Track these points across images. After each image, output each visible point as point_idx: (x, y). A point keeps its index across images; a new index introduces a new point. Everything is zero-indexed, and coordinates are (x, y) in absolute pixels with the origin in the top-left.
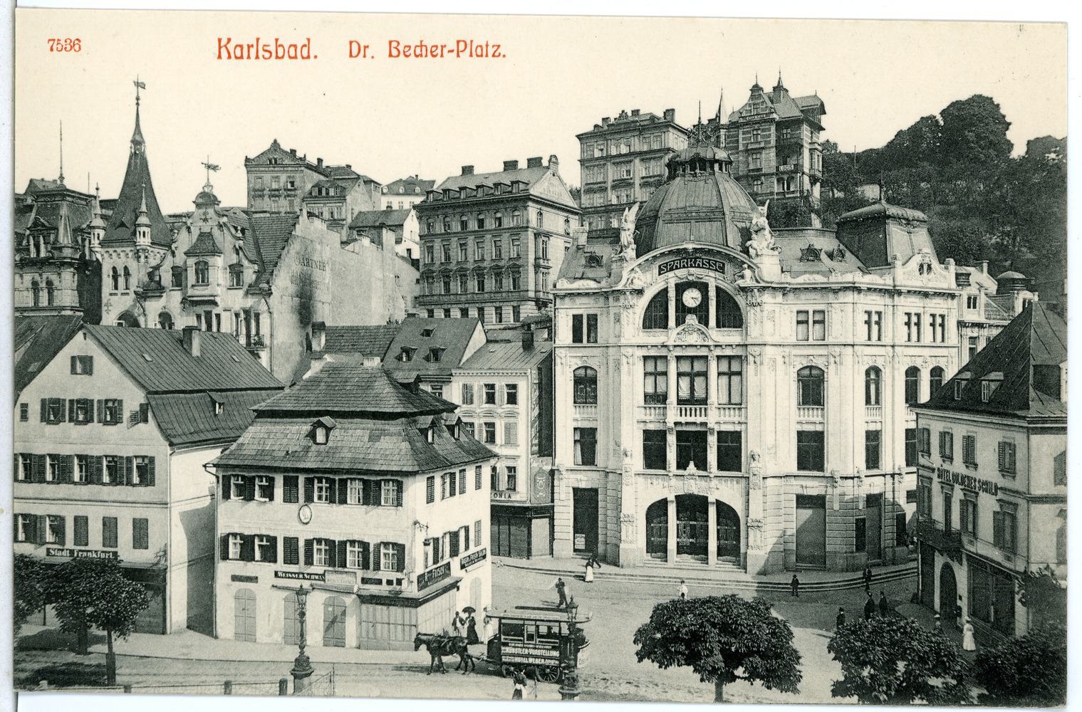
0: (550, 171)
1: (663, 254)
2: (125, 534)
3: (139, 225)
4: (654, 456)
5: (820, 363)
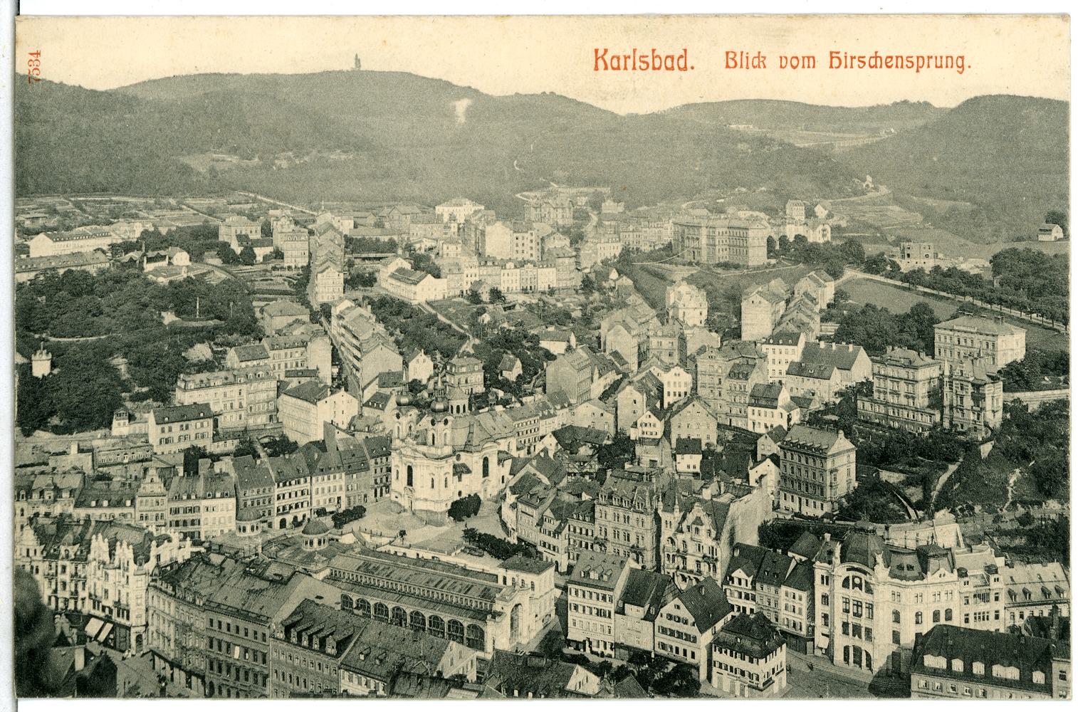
2: (689, 654)
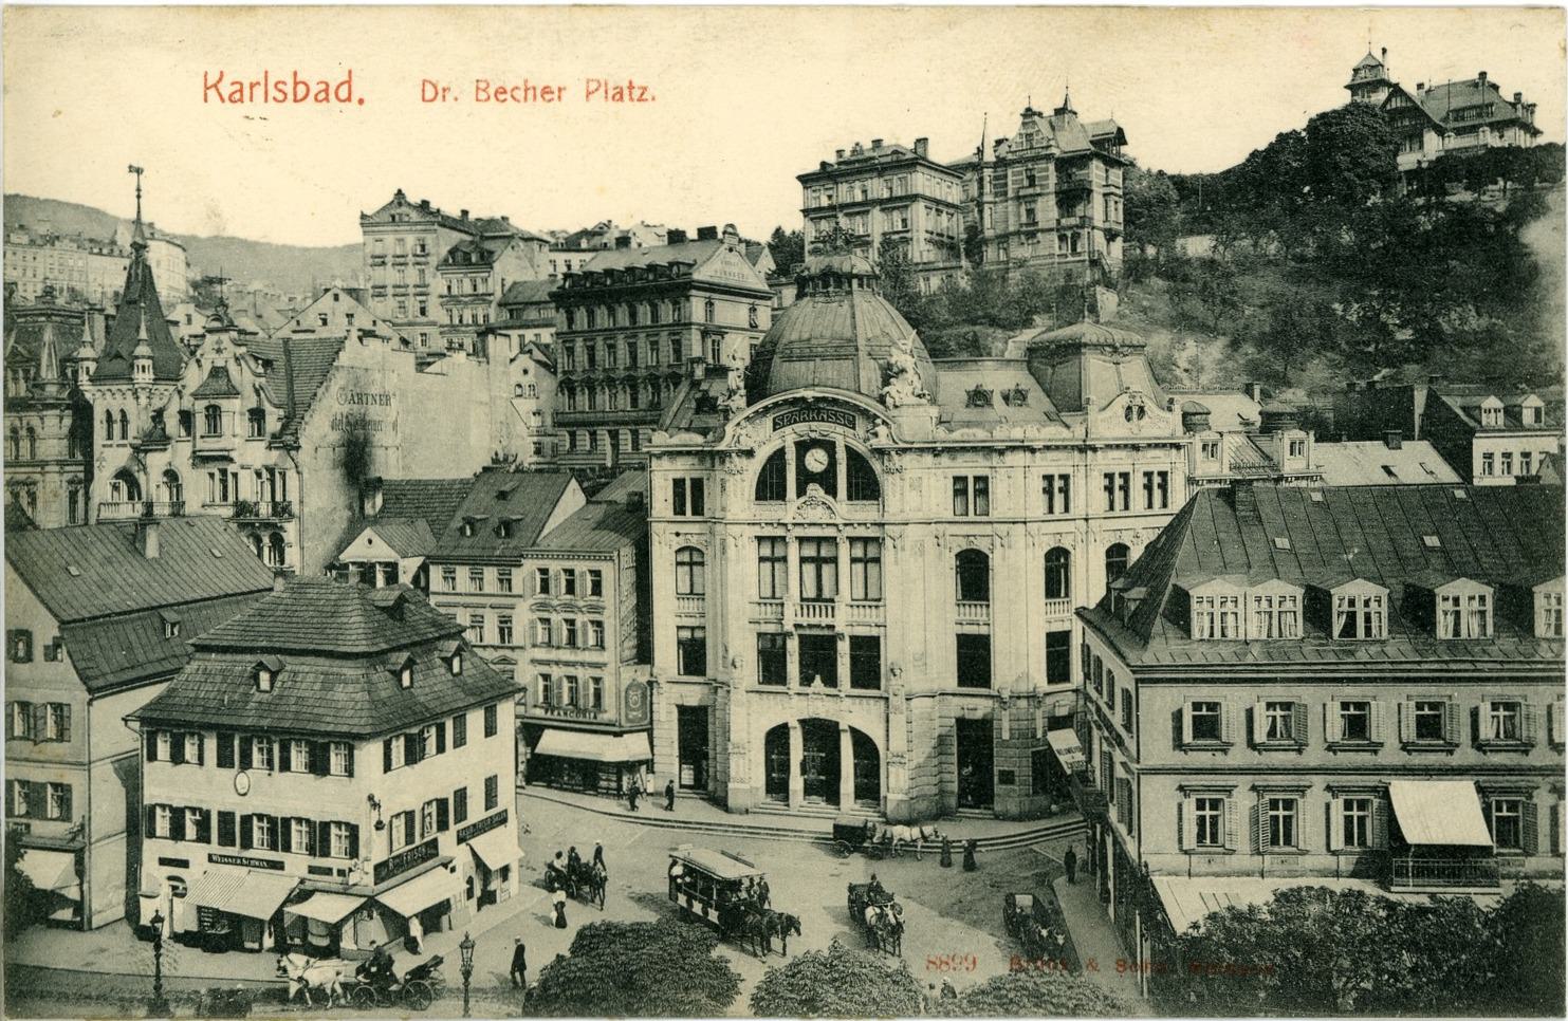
0: (726, 246)
1: (776, 405)
3: (137, 358)
4: (772, 667)
5: (982, 545)
